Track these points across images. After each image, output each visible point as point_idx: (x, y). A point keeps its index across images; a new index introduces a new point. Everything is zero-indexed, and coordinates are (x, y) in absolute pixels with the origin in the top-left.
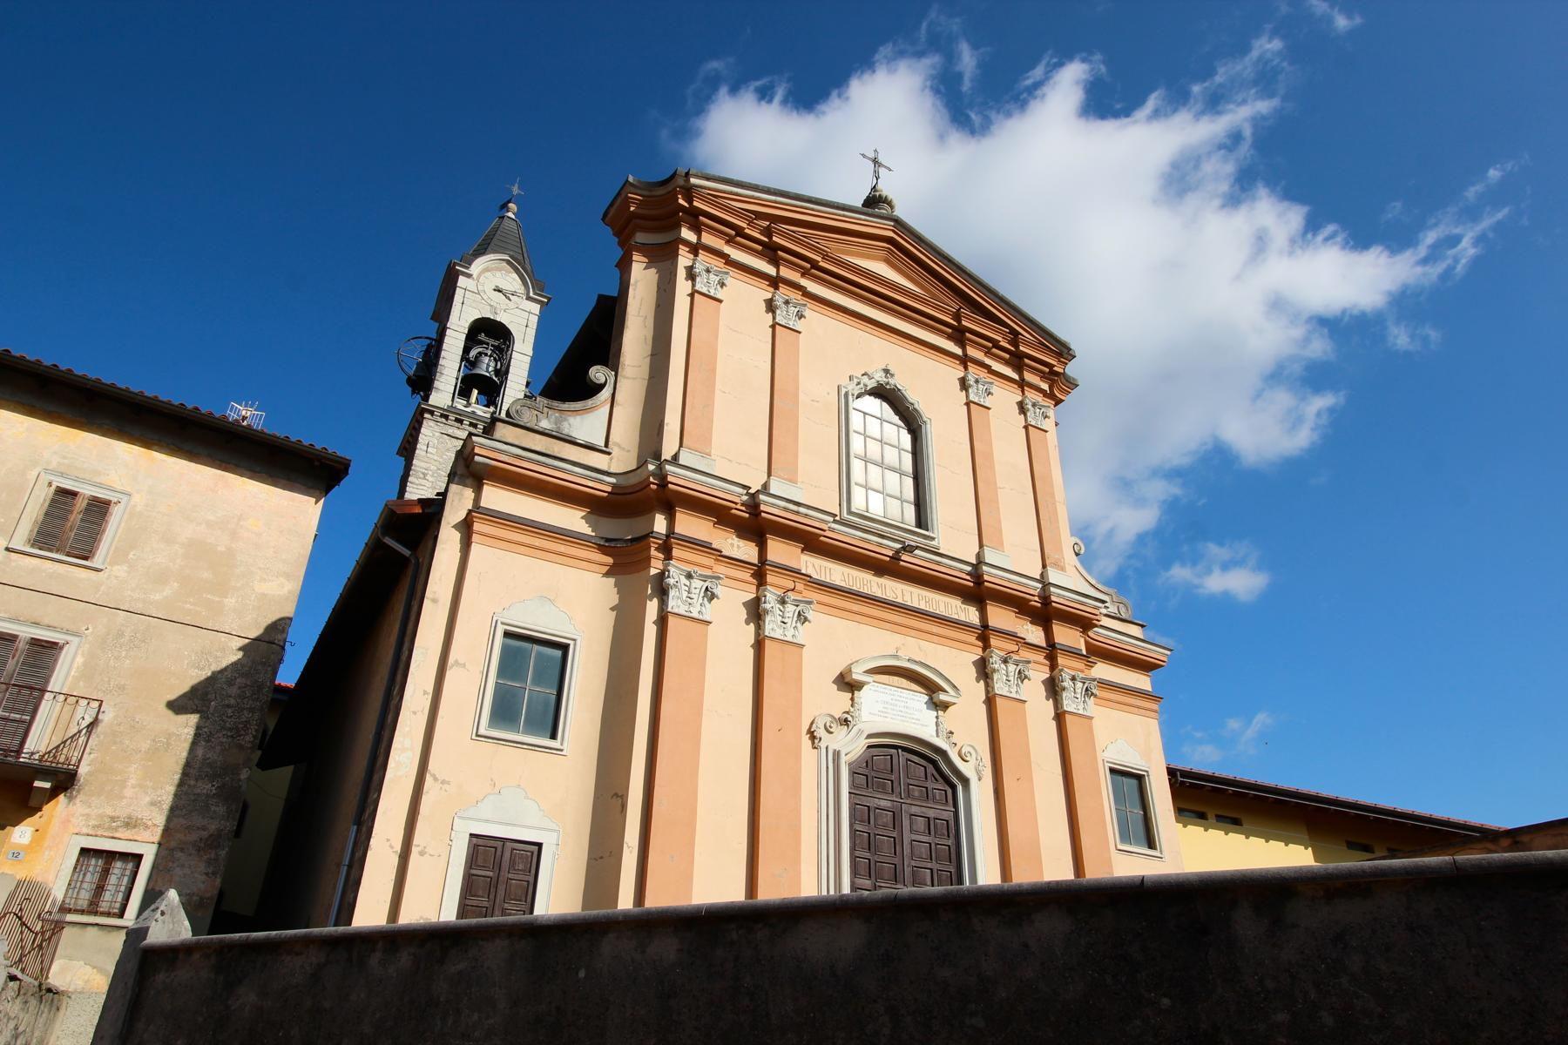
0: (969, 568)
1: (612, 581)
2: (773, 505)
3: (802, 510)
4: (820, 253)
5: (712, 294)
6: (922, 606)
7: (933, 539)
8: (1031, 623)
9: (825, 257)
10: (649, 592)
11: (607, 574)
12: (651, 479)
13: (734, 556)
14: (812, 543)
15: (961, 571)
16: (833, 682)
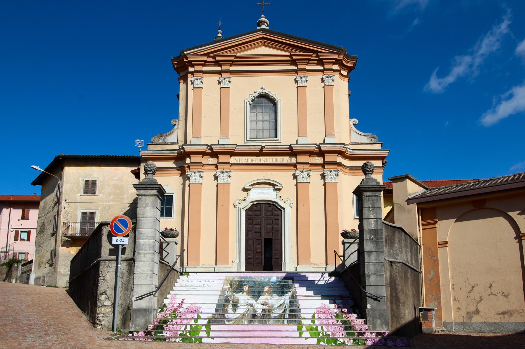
0: (288, 147)
2: (216, 147)
4: (234, 57)
5: (199, 87)
6: (274, 162)
7: (278, 140)
8: (318, 157)
10: (186, 179)
12: (182, 150)
14: (232, 154)
15: (285, 148)
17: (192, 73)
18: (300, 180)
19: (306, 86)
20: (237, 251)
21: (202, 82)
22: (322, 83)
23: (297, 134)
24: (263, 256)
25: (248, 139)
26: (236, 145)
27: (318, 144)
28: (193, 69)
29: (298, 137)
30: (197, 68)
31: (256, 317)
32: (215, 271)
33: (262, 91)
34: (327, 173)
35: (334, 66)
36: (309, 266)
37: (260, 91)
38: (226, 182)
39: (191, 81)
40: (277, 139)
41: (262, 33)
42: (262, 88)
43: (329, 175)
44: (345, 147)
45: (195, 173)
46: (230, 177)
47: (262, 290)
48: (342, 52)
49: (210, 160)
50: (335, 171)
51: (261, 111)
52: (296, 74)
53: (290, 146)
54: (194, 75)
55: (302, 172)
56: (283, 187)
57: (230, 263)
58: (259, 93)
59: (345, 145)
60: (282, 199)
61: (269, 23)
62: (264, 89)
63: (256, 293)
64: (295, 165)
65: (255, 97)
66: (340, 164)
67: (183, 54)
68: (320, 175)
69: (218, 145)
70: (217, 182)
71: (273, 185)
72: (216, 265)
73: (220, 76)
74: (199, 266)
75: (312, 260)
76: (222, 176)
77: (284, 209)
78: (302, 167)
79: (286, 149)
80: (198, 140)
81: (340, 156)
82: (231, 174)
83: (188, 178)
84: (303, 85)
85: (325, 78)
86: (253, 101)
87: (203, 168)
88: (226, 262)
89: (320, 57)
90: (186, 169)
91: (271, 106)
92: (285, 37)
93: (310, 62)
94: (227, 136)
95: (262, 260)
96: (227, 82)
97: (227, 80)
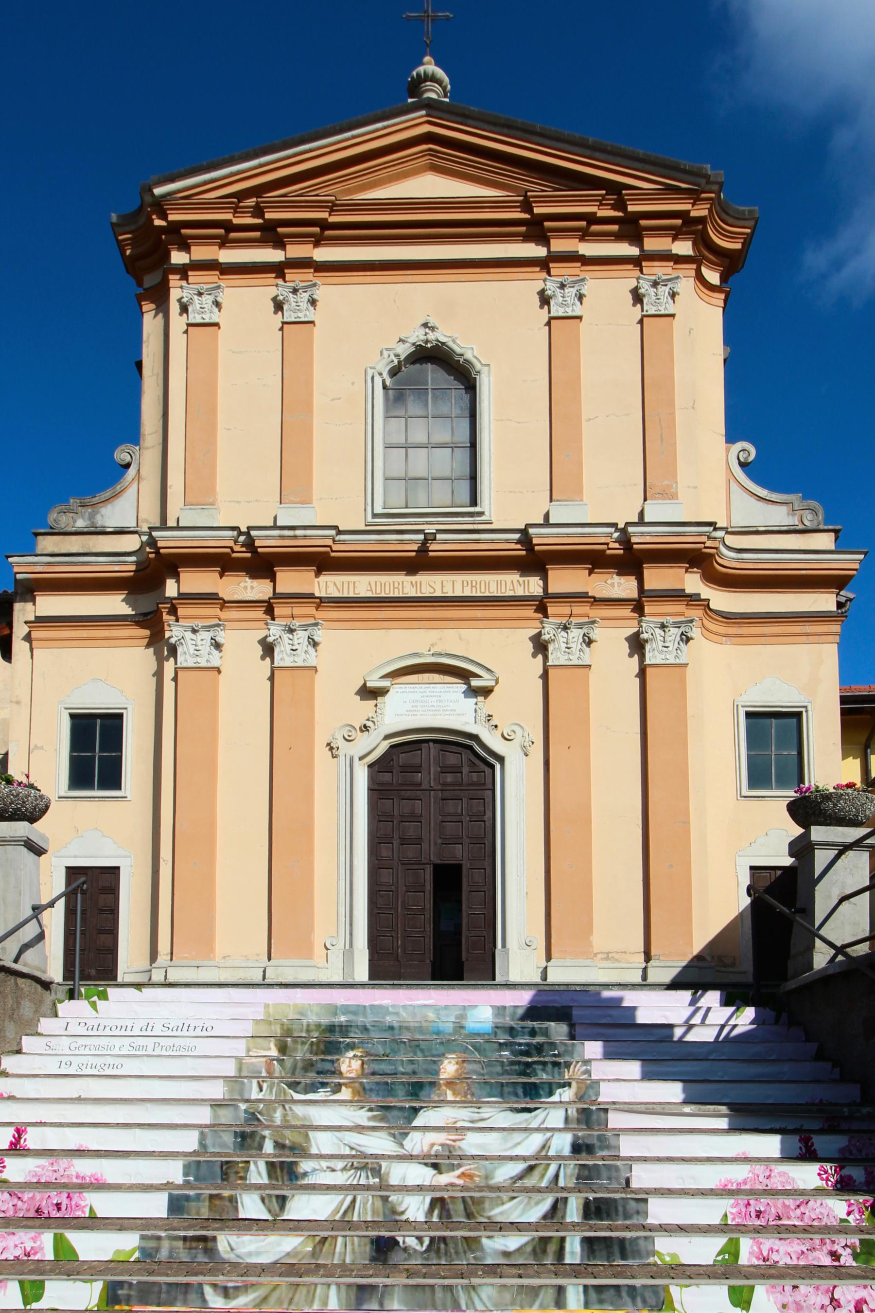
0: (517, 536)
1: (151, 650)
2: (267, 537)
3: (299, 532)
5: (207, 321)
6: (468, 593)
7: (481, 514)
8: (619, 574)
9: (333, 208)
10: (166, 653)
11: (148, 646)
12: (148, 550)
13: (247, 599)
15: (507, 541)
16: (357, 694)
17: (183, 271)
18: (556, 656)
19: (580, 318)
20: (342, 910)
21: (217, 304)
22: (634, 305)
23: (549, 492)
24: (430, 928)
25: (379, 510)
26: (335, 527)
27: (621, 525)
28: (188, 256)
29: (551, 501)
30: (201, 253)
31: (396, 1257)
32: (267, 981)
33: (426, 334)
34: (650, 631)
35: (676, 243)
36: (588, 962)
37: (417, 336)
38: (302, 664)
39: (179, 300)
40: (477, 509)
41: (427, 115)
42: (425, 325)
43: (659, 638)
44: (715, 539)
45: (194, 631)
46: (315, 644)
47: (427, 1071)
48: (708, 188)
49: (245, 588)
50: (677, 625)
51: (421, 412)
52: (544, 275)
53: (524, 532)
54: (191, 279)
55: (565, 628)
56: (497, 682)
57: (319, 950)
58: (414, 344)
59: (715, 529)
60: (496, 726)
61: (449, 87)
62: (433, 329)
63: (401, 1092)
64: (541, 606)
65: (402, 358)
66: (693, 599)
67: (148, 199)
68: (627, 639)
69: (275, 527)
70: (272, 662)
71: (463, 675)
72: (269, 959)
73: (280, 282)
74: (211, 963)
75: (599, 941)
76: (287, 641)
77: (501, 759)
78: (565, 609)
79: (509, 545)
80: (206, 512)
81: (695, 570)
82: (319, 635)
83: (173, 651)
84: (570, 314)
85: (645, 287)
86: (394, 372)
87: (224, 615)
88: (305, 949)
89: (630, 208)
90: (165, 617)
91: (457, 393)
92: (506, 131)
93: (595, 228)
94: (306, 501)
95: (427, 940)
96: (304, 305)
97: (306, 296)
